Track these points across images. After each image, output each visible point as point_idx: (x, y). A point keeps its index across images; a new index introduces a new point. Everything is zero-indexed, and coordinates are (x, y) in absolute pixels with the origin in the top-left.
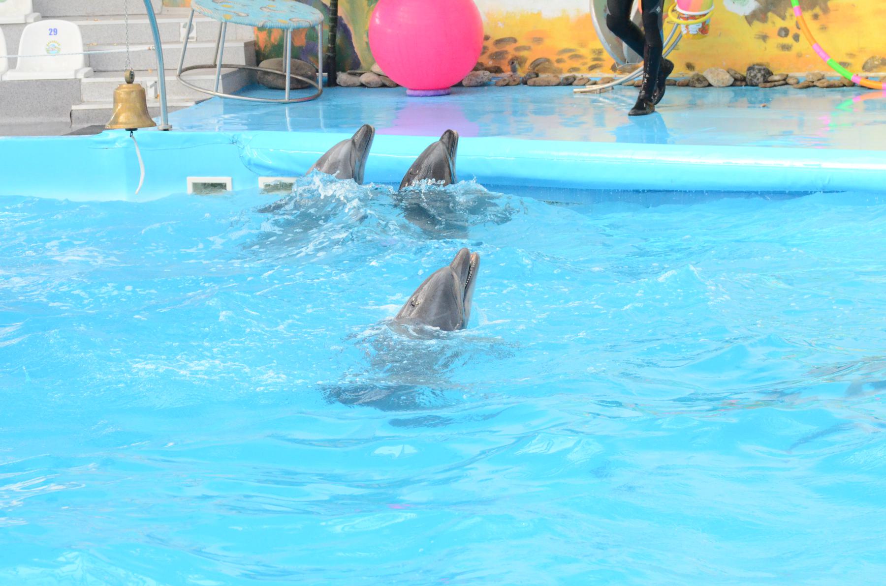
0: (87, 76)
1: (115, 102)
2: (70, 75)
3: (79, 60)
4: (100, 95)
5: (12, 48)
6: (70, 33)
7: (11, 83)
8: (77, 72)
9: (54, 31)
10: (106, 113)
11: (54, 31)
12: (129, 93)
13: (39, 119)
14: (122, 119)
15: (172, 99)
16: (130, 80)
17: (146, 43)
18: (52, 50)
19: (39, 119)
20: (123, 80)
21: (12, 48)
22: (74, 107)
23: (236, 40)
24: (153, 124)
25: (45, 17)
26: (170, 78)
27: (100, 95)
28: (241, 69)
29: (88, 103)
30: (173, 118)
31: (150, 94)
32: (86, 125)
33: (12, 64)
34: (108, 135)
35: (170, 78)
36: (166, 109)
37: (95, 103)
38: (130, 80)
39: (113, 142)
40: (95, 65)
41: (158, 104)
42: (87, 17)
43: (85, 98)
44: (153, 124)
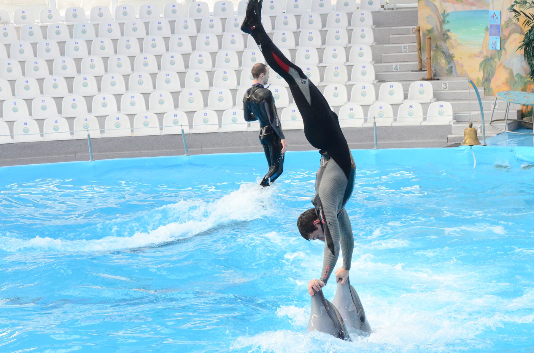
0: (454, 124)
1: (465, 134)
2: (447, 123)
3: (451, 118)
4: (459, 131)
5: (425, 113)
6: (448, 107)
7: (425, 126)
8: (450, 122)
9: (442, 106)
10: (461, 139)
11: (442, 106)
12: (471, 131)
13: (434, 140)
14: (467, 141)
15: (487, 133)
16: (471, 126)
17: (478, 111)
18: (441, 114)
19: (434, 140)
20: (468, 125)
21: (425, 113)
22: (448, 136)
23: (514, 109)
24: (480, 144)
25: (438, 100)
26: (487, 125)
27: (459, 131)
28: (515, 121)
29: (454, 134)
30: (488, 141)
31: (479, 131)
32: (453, 143)
33: (425, 119)
34: (461, 148)
35: (487, 125)
36: (485, 137)
37: (457, 134)
38: (471, 126)
39: (464, 150)
40: (458, 120)
41: (482, 135)
42: (455, 100)
43: (453, 132)
44: (480, 144)
